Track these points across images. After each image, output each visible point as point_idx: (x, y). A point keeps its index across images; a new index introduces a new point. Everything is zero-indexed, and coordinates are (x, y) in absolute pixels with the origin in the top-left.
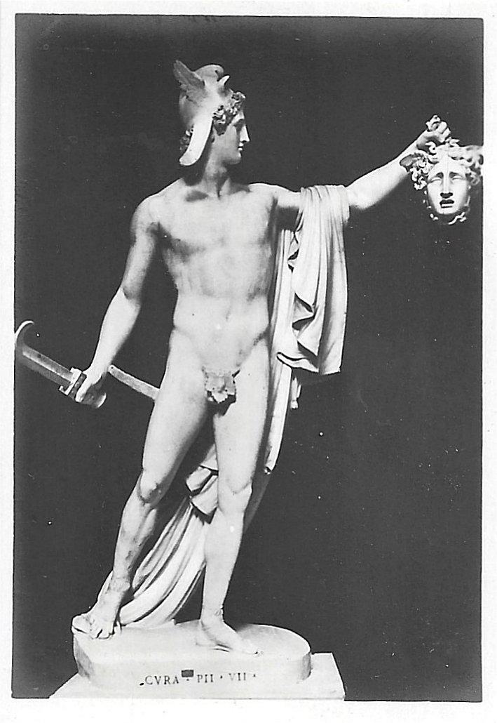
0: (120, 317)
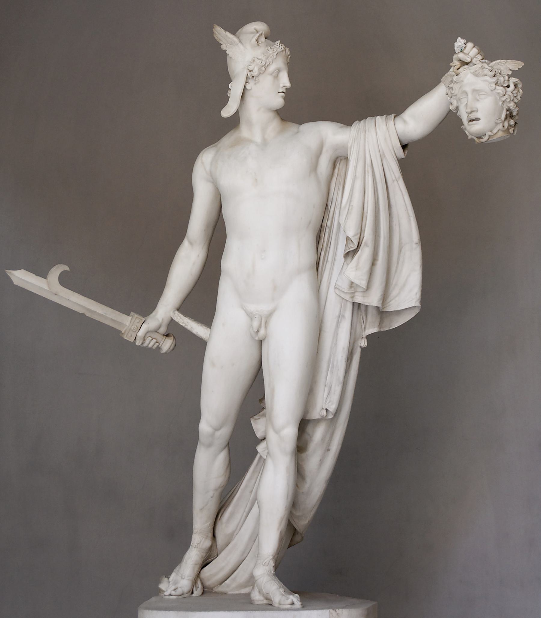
0: (186, 263)
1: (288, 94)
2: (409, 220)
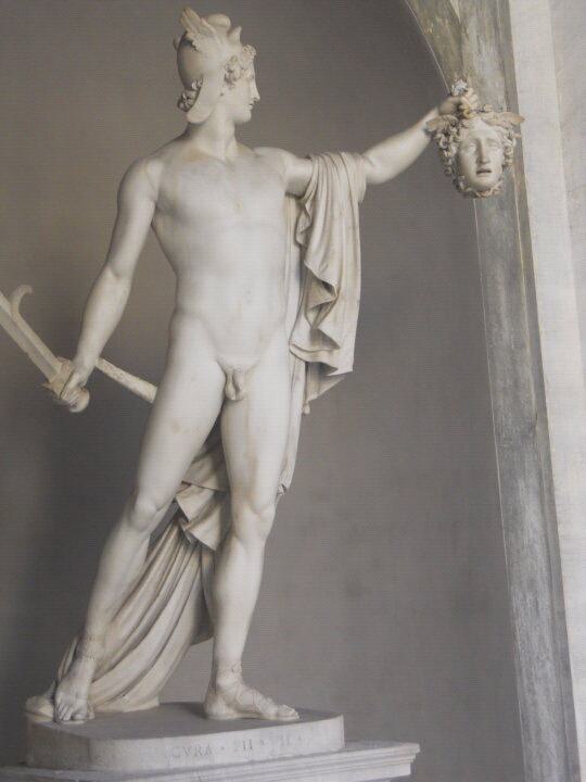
1: (257, 108)
2: (356, 274)
